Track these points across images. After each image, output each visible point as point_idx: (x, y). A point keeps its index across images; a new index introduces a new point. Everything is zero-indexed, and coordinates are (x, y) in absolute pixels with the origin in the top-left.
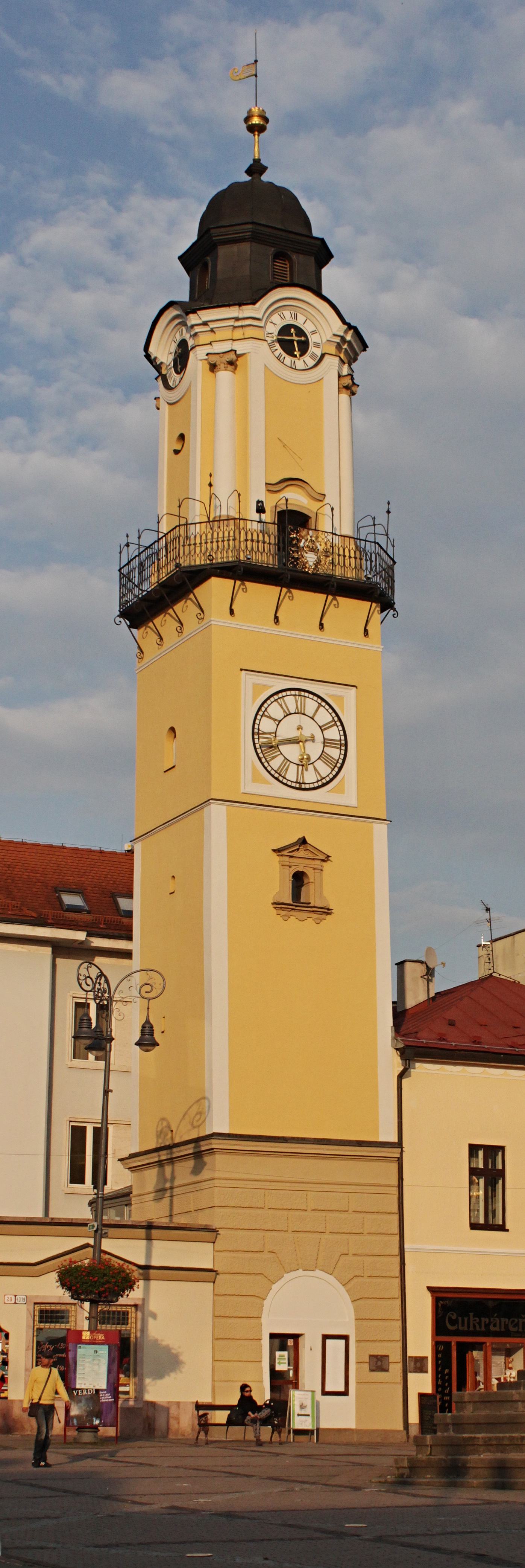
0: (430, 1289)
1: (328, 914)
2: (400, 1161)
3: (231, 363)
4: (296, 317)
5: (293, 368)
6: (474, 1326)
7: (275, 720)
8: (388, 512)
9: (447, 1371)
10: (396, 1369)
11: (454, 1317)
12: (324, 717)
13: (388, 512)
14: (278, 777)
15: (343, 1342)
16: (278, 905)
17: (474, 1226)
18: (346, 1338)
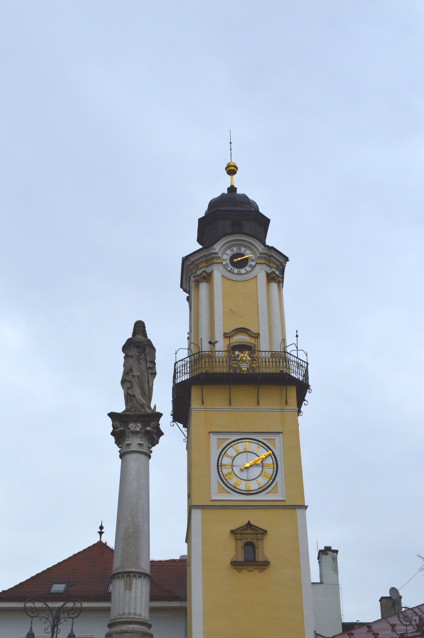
4: (240, 249)
5: (239, 274)
16: (235, 564)
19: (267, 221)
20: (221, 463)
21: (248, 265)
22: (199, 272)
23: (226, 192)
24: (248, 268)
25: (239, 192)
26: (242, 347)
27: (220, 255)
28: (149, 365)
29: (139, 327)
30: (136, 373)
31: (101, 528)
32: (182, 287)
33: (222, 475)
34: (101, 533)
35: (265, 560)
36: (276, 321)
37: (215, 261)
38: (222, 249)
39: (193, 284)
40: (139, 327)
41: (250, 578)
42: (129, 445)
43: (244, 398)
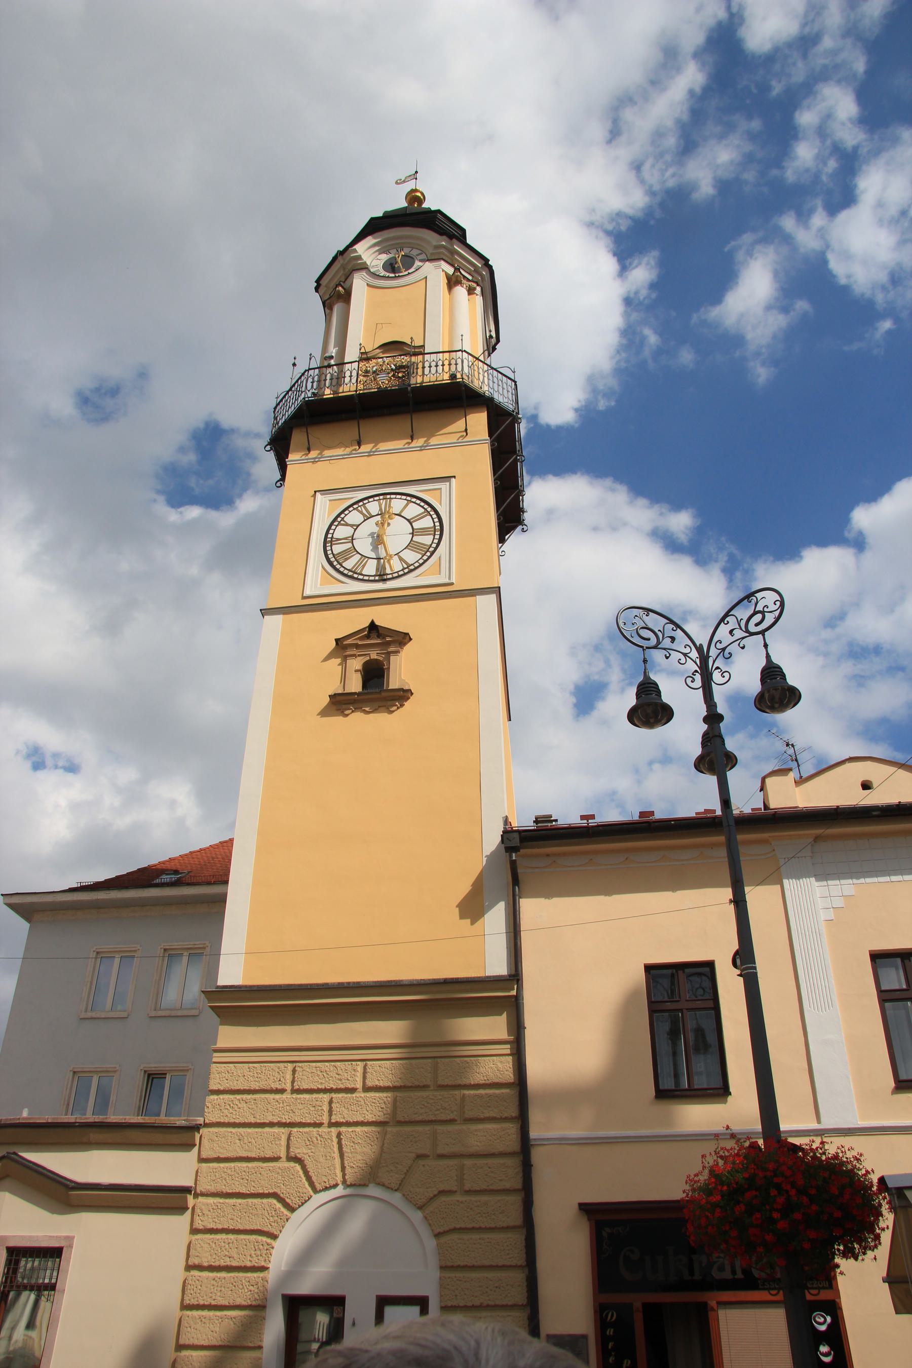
7: (352, 526)
12: (414, 510)
14: (354, 575)
20: (332, 537)
33: (331, 556)
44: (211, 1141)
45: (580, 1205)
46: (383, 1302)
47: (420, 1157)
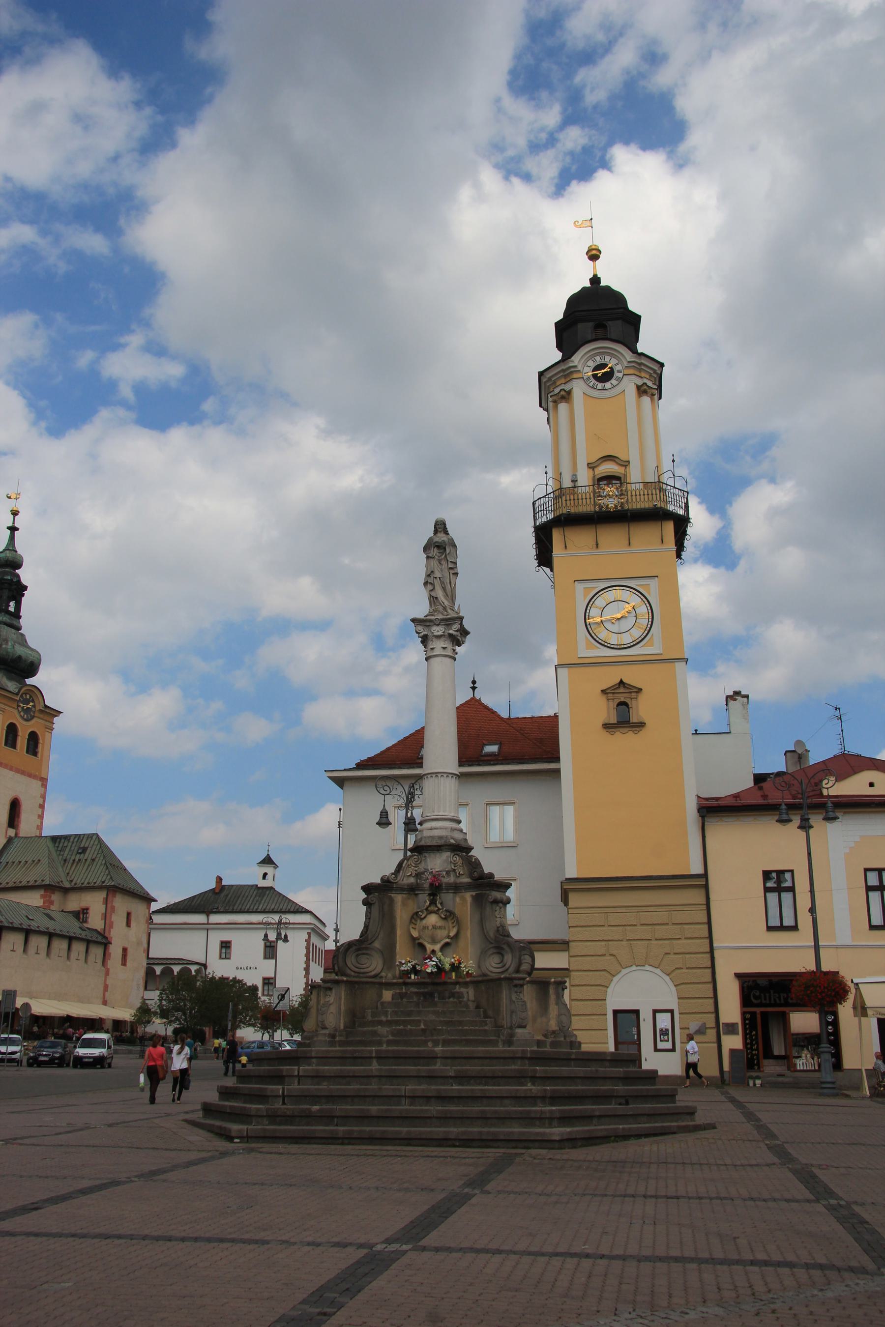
0: (738, 976)
1: (606, 724)
2: (706, 887)
3: (563, 398)
4: (604, 359)
6: (775, 1000)
8: (673, 461)
9: (754, 1033)
10: (711, 1034)
11: (758, 994)
12: (635, 600)
13: (673, 461)
15: (669, 1014)
16: (607, 726)
17: (770, 929)
18: (672, 1012)
19: (639, 317)
21: (614, 377)
22: (557, 391)
23: (588, 285)
24: (614, 381)
25: (603, 283)
26: (609, 479)
27: (580, 368)
28: (451, 565)
29: (440, 527)
30: (438, 574)
31: (474, 682)
32: (541, 406)
34: (474, 688)
35: (641, 721)
36: (650, 443)
37: (575, 376)
38: (584, 360)
39: (551, 405)
40: (440, 527)
41: (624, 739)
42: (432, 649)
43: (612, 538)
44: (575, 948)
45: (735, 974)
46: (655, 1012)
47: (667, 954)
